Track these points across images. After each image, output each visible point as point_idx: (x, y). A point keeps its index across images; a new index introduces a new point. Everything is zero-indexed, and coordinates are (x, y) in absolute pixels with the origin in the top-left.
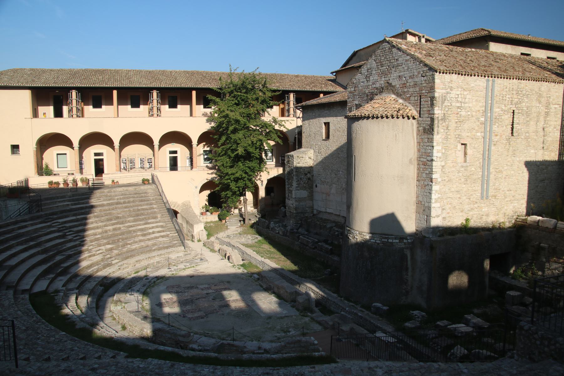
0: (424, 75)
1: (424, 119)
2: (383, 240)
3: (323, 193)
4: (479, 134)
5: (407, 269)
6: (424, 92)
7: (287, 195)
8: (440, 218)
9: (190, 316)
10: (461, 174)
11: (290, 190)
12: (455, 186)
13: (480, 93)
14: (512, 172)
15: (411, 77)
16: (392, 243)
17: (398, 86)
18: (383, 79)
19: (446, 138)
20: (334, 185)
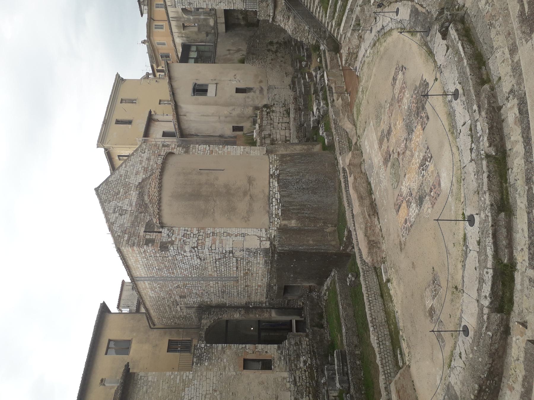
0: (143, 152)
6: (156, 152)
15: (141, 164)
17: (144, 176)
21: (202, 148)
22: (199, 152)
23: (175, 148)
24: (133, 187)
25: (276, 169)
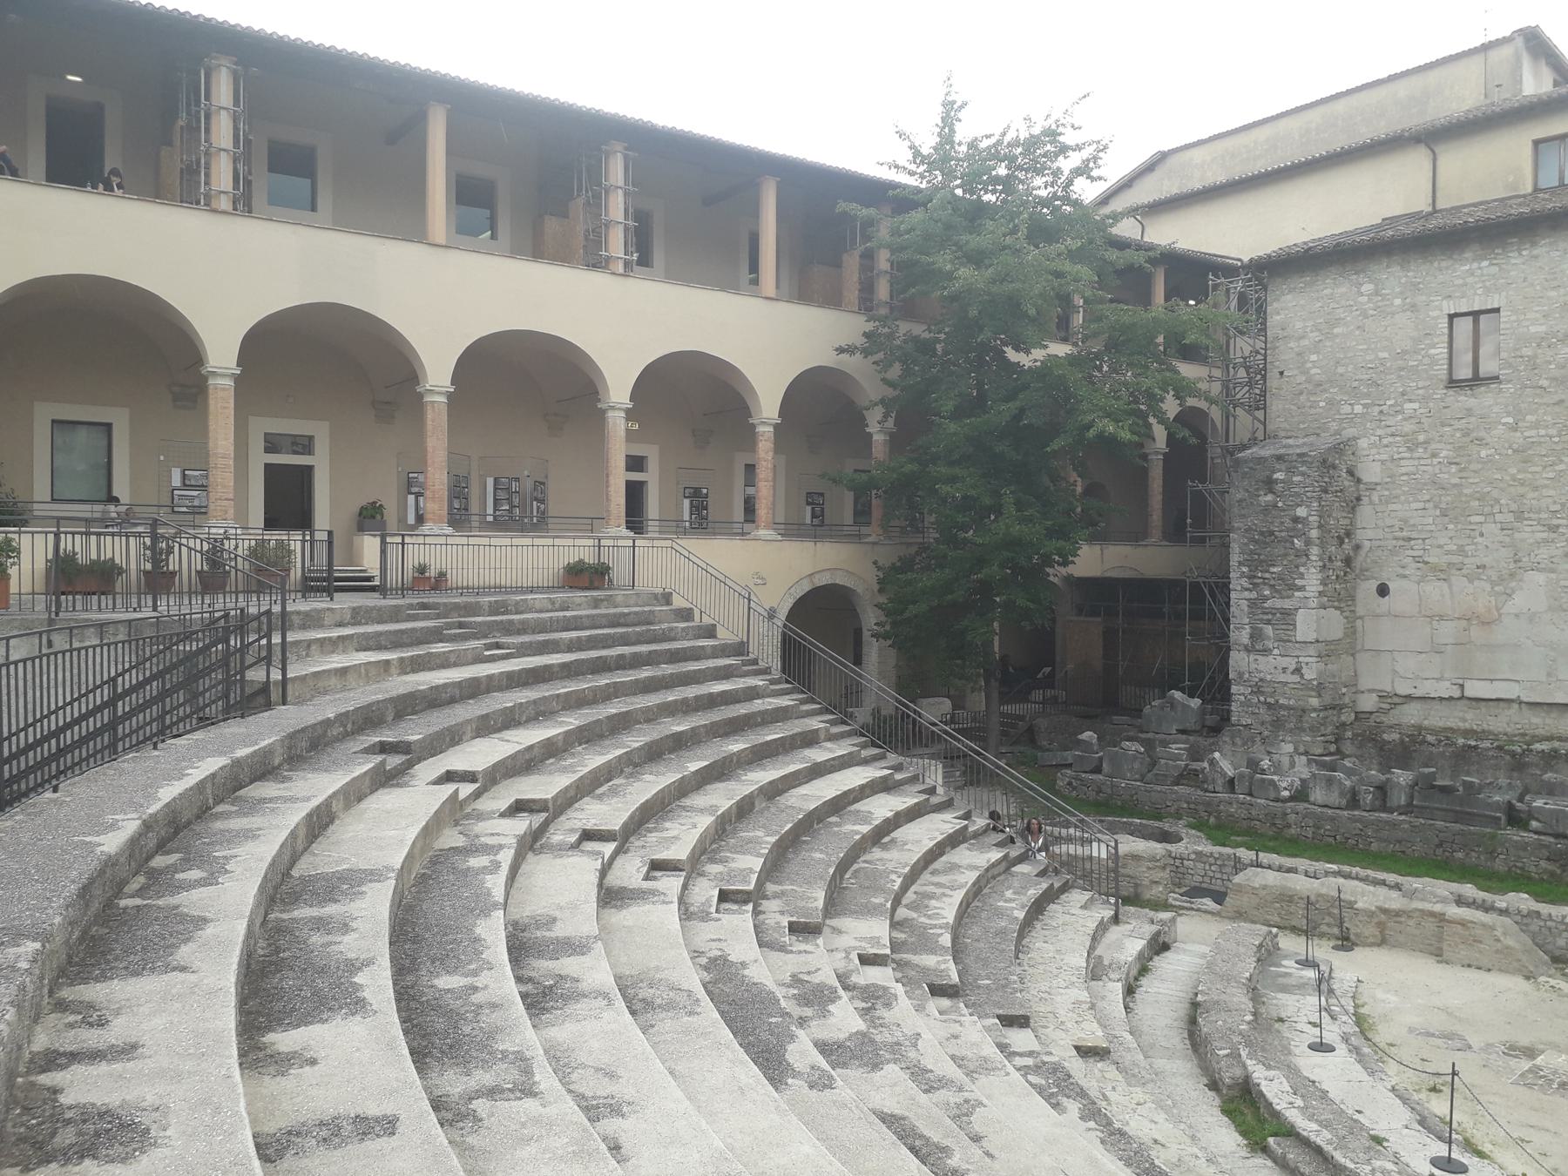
3: (1441, 618)
20: (1540, 578)
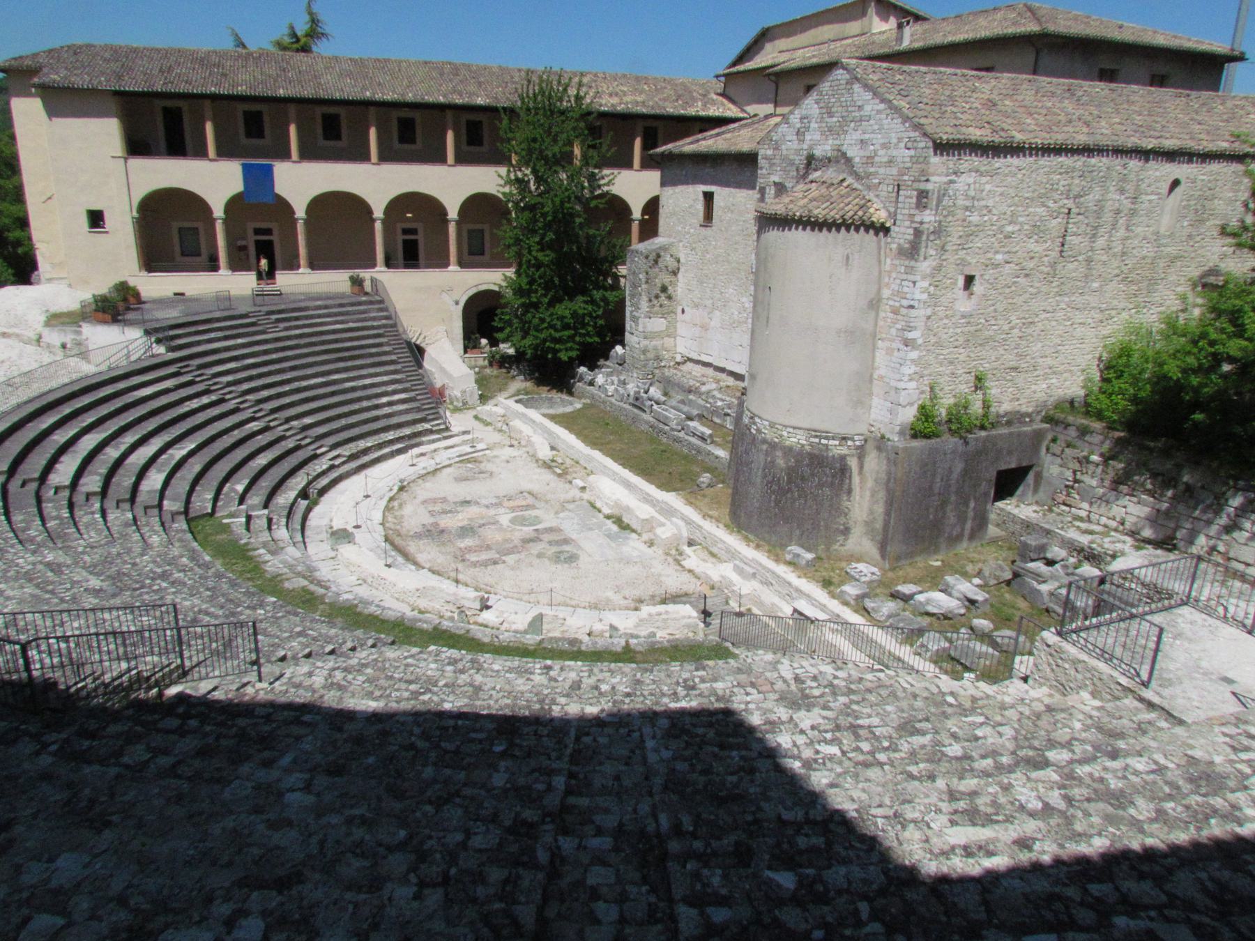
0: (909, 145)
1: (902, 230)
2: (813, 440)
4: (999, 257)
5: (850, 492)
6: (906, 178)
7: (628, 327)
8: (916, 406)
9: (473, 558)
10: (959, 331)
11: (634, 317)
12: (945, 352)
13: (1009, 179)
14: (1054, 323)
15: (885, 146)
16: (827, 445)
17: (857, 160)
18: (830, 142)
19: (938, 268)
21: (906, 289)
22: (898, 281)
23: (912, 222)
24: (837, 142)
25: (758, 430)
